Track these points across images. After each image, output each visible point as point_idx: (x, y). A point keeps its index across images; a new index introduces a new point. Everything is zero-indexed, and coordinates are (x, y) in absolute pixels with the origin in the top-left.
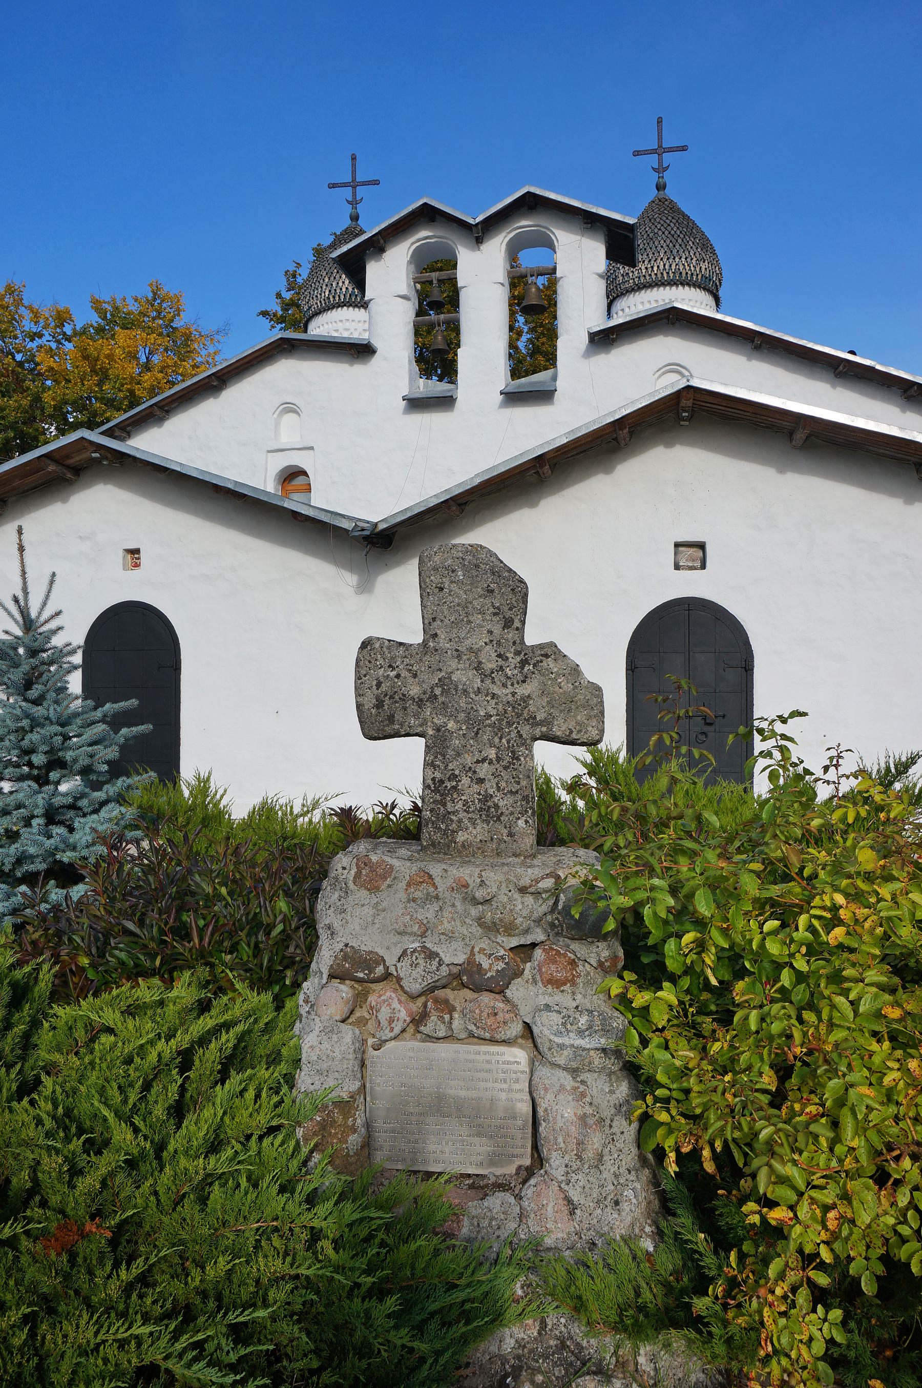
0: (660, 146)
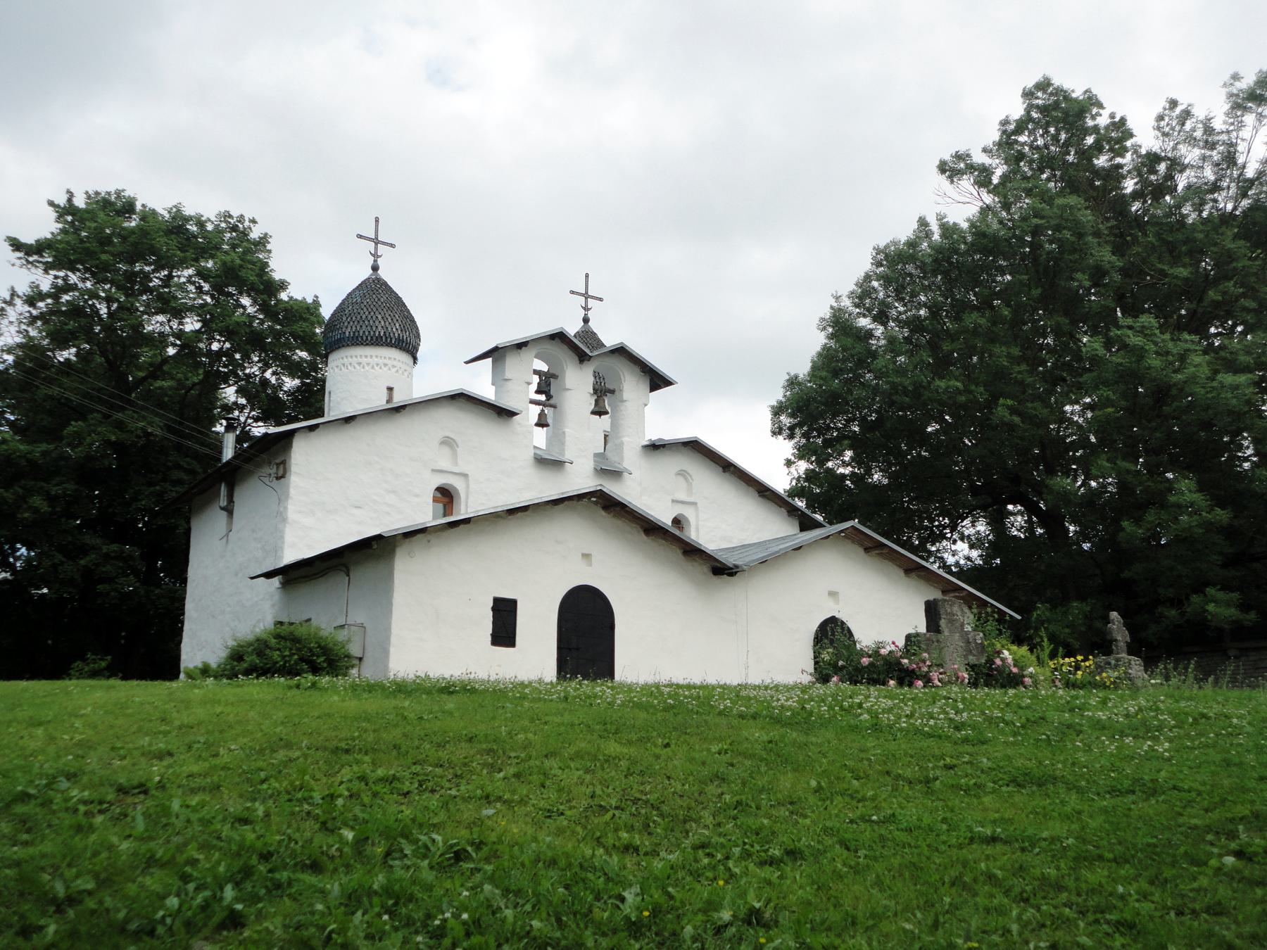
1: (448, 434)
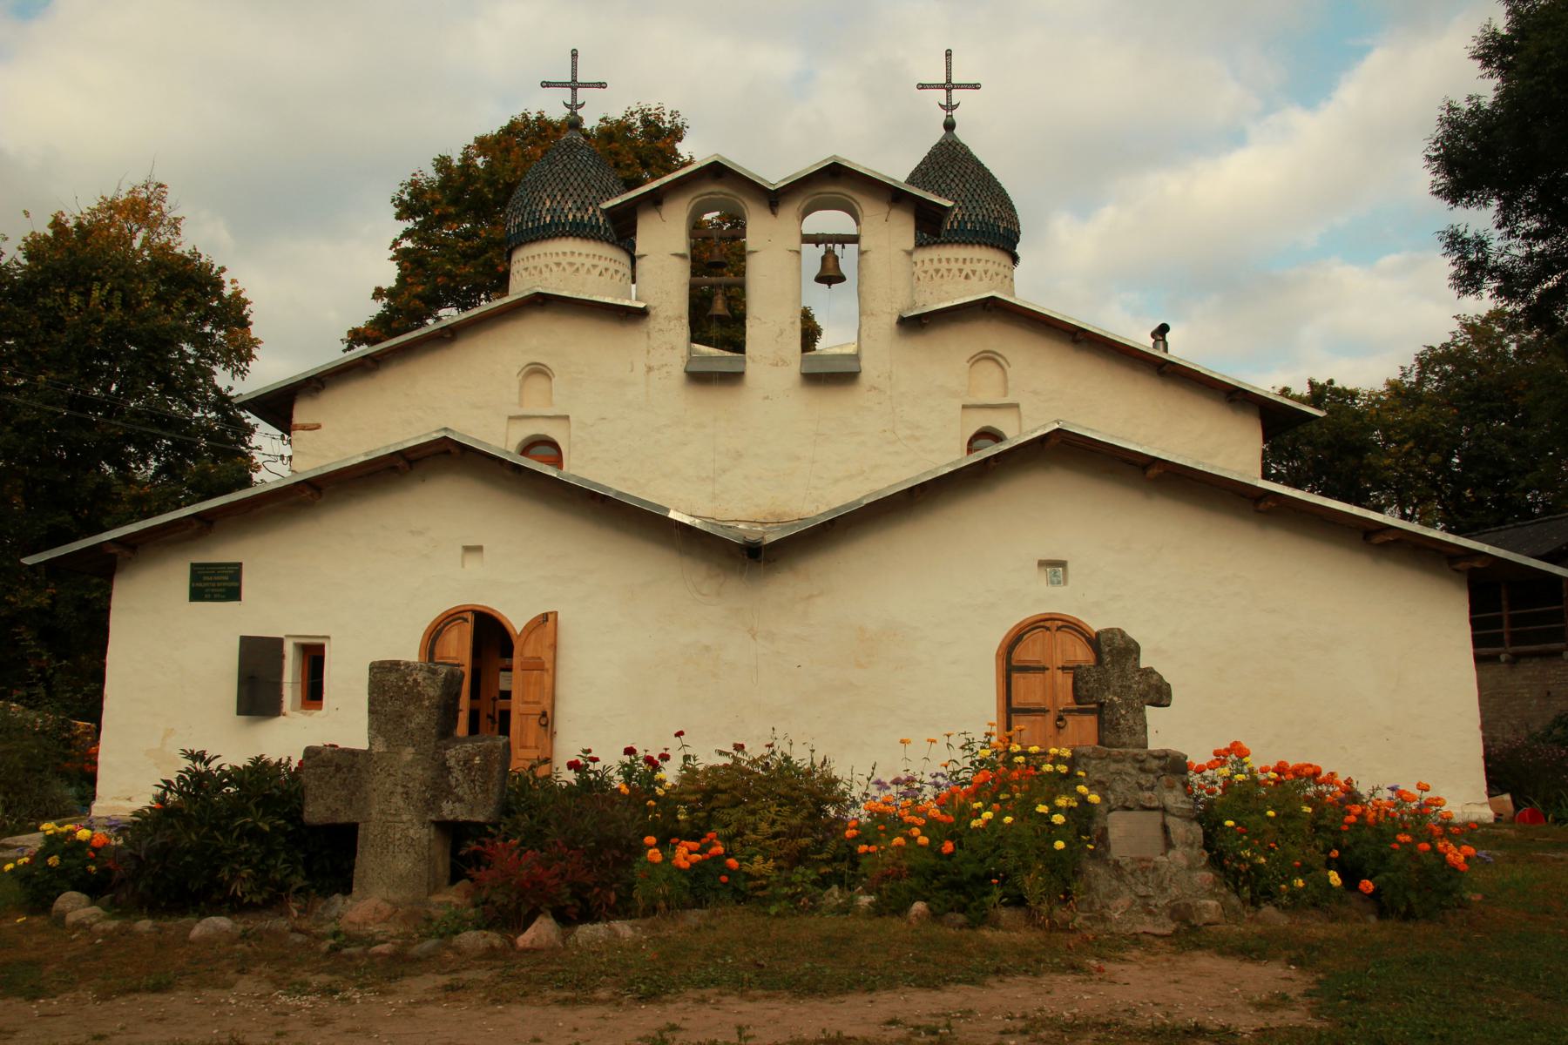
0: (949, 81)
1: (524, 362)
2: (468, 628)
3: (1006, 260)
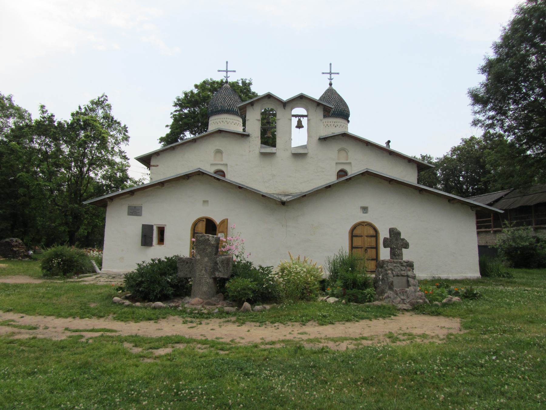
2: (204, 223)
3: (346, 122)
